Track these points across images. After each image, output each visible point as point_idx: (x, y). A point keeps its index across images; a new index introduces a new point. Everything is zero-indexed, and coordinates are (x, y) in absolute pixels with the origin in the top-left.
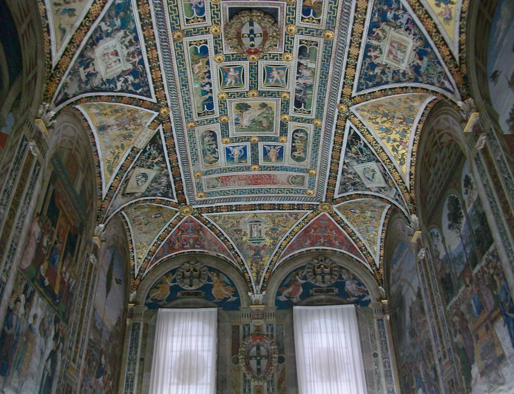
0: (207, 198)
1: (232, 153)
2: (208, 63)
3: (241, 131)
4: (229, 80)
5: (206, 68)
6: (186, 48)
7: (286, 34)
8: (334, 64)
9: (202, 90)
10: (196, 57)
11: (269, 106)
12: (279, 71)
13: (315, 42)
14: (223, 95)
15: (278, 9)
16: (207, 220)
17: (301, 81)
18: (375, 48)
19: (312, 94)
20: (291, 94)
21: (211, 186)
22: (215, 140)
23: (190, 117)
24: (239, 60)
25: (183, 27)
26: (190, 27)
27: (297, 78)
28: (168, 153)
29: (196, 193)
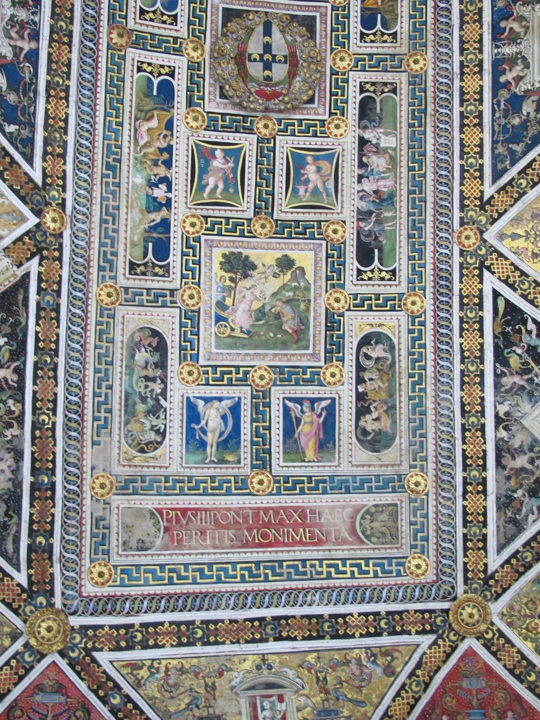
0: (119, 591)
1: (203, 423)
2: (169, 126)
3: (229, 347)
4: (212, 181)
5: (165, 136)
6: (130, 73)
8: (436, 127)
9: (148, 196)
10: (149, 104)
12: (321, 163)
13: (391, 84)
15: (315, 17)
16: (109, 678)
17: (368, 186)
18: (512, 61)
19: (395, 218)
21: (133, 543)
22: (162, 364)
24: (236, 132)
25: (131, 25)
26: (144, 28)
28: (36, 367)
29: (86, 562)
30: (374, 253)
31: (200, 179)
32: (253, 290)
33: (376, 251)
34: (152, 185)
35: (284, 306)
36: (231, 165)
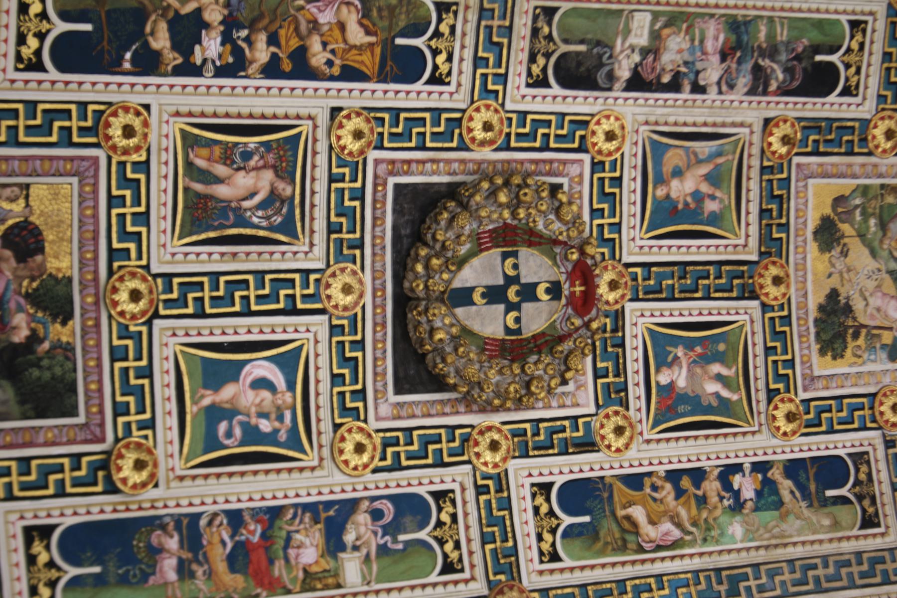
2: (634, 481)
4: (712, 387)
5: (655, 488)
6: (567, 575)
7: (508, 148)
9: (756, 509)
10: (608, 528)
11: (828, 211)
12: (667, 169)
13: (535, 18)
14: (780, 414)
15: (397, 186)
17: (712, 73)
19: (771, 19)
20: (771, 114)
23: (882, 561)
24: (622, 345)
26: (478, 559)
27: (698, 89)
30: (820, 62)
31: (709, 410)
32: (867, 294)
33: (818, 58)
34: (738, 506)
35: (889, 234)
36: (680, 351)
